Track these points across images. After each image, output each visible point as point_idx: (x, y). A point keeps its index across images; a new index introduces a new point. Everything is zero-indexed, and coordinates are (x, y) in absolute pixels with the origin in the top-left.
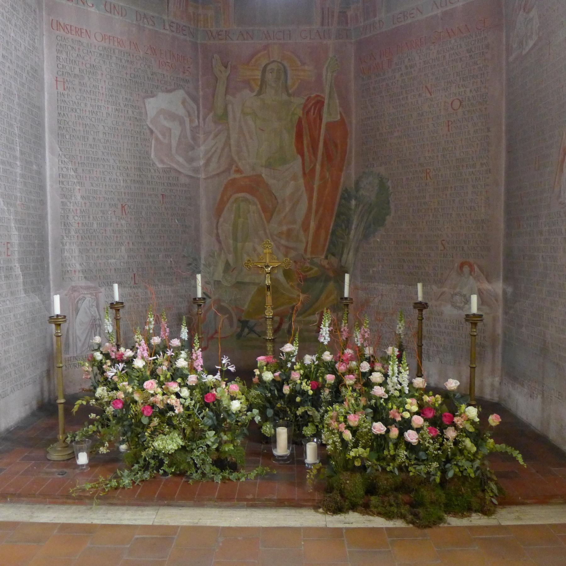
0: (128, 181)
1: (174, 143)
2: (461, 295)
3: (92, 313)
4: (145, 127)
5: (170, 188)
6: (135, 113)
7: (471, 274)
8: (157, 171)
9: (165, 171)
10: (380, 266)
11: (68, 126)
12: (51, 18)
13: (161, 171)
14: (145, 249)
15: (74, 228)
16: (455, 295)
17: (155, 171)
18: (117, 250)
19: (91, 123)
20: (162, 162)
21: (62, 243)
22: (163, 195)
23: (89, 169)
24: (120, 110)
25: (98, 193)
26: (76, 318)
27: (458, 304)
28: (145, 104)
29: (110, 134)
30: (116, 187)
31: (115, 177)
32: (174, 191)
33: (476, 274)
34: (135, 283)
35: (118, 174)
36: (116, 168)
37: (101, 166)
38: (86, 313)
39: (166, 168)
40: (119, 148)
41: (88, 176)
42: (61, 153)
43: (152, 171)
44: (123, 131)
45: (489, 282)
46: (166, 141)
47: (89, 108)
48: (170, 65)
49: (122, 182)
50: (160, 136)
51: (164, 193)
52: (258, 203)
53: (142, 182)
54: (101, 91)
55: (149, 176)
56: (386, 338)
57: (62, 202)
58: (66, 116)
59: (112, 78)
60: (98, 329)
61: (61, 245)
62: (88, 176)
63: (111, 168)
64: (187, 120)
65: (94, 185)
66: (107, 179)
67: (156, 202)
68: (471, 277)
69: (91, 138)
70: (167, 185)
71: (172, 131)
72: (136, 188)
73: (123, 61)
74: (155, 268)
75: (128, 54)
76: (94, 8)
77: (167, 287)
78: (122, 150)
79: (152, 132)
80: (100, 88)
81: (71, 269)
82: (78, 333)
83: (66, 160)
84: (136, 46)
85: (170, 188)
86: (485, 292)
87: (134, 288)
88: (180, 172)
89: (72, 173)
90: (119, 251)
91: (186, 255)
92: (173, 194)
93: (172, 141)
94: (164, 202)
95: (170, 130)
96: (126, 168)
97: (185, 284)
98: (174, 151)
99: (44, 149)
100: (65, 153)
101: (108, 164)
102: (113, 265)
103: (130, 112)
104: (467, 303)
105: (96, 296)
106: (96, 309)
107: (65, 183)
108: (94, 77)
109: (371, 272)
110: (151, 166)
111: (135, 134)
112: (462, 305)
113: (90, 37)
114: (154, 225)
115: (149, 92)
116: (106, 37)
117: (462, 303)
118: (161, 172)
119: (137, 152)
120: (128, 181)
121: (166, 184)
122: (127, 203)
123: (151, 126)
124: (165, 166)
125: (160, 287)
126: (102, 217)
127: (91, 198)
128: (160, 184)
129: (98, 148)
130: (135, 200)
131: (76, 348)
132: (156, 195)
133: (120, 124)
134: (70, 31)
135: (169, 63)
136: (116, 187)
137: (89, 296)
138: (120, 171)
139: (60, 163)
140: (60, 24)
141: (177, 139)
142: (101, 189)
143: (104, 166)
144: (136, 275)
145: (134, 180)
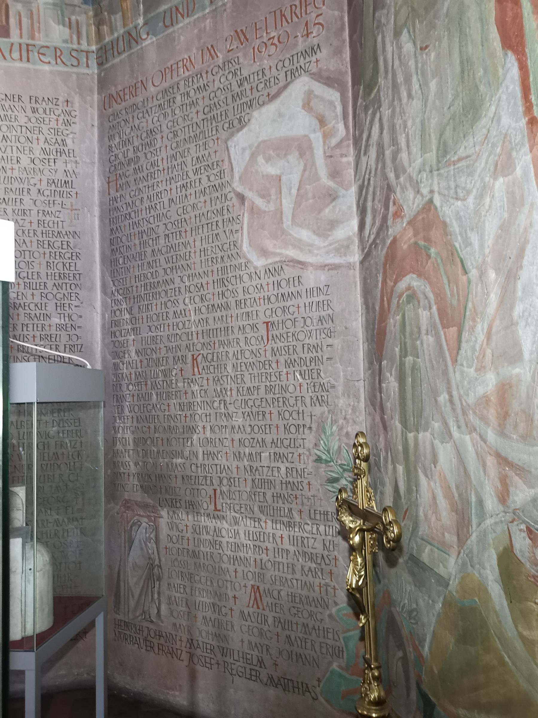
0: (204, 310)
1: (287, 205)
3: (150, 551)
4: (232, 194)
5: (282, 304)
6: (212, 178)
8: (254, 276)
9: (268, 271)
11: (121, 244)
12: (103, 95)
13: (263, 273)
14: (233, 440)
15: (127, 403)
17: (251, 277)
18: (185, 440)
19: (149, 225)
20: (264, 253)
21: (114, 428)
22: (267, 323)
23: (146, 303)
24: (189, 185)
25: (158, 341)
26: (129, 554)
28: (228, 150)
29: (174, 234)
30: (184, 325)
31: (182, 306)
32: (292, 309)
34: (216, 509)
35: (187, 301)
36: (183, 290)
37: (163, 294)
38: (142, 549)
39: (271, 264)
40: (187, 254)
41: (144, 315)
42: (114, 288)
43: (246, 278)
44: (193, 220)
46: (272, 207)
47: (147, 204)
48: (276, 41)
49: (192, 313)
50: (259, 202)
51: (271, 319)
52: (431, 296)
53: (228, 307)
54: (161, 168)
55: (240, 291)
57: (114, 364)
58: (119, 230)
59: (175, 135)
60: (157, 585)
61: (113, 432)
62: (144, 315)
63: (177, 293)
64: (317, 138)
65: (153, 329)
66: (171, 315)
67: (253, 341)
69: (149, 250)
70: (277, 299)
71: (284, 178)
72: (217, 319)
73: (192, 93)
74: (253, 481)
75: (199, 76)
76: (149, 37)
77: (278, 526)
78: (192, 255)
79: (242, 198)
80: (160, 163)
81: (125, 471)
82: (132, 581)
83: (120, 297)
84: (212, 51)
85: (282, 304)
87: (214, 518)
88: (302, 264)
89: (127, 316)
90: (189, 443)
91: (324, 457)
92: (290, 316)
93: (284, 201)
94: (270, 338)
95: (279, 178)
96: (199, 286)
97: (322, 528)
98: (287, 222)
99: (91, 289)
100: (119, 288)
101: (172, 286)
102: (179, 469)
103: (205, 180)
105: (154, 522)
106: (155, 546)
107: (118, 334)
108: (151, 150)
110: (243, 268)
111: (213, 216)
113: (146, 89)
114: (249, 389)
115: (236, 122)
116: (167, 70)
118: (262, 276)
119: (218, 251)
120: (204, 310)
121: (273, 299)
122: (202, 352)
123: (240, 189)
124: (270, 261)
125: (263, 524)
126: (163, 381)
127: (149, 351)
128: (262, 301)
129: (158, 264)
130: (214, 344)
131: (128, 608)
132: (254, 327)
133: (189, 208)
134: (122, 97)
135: (273, 38)
136: (184, 325)
137: (146, 520)
138: (191, 294)
139: (113, 304)
140: (112, 96)
141: (294, 191)
142: (162, 334)
143: (166, 292)
144: (218, 491)
145: (213, 306)
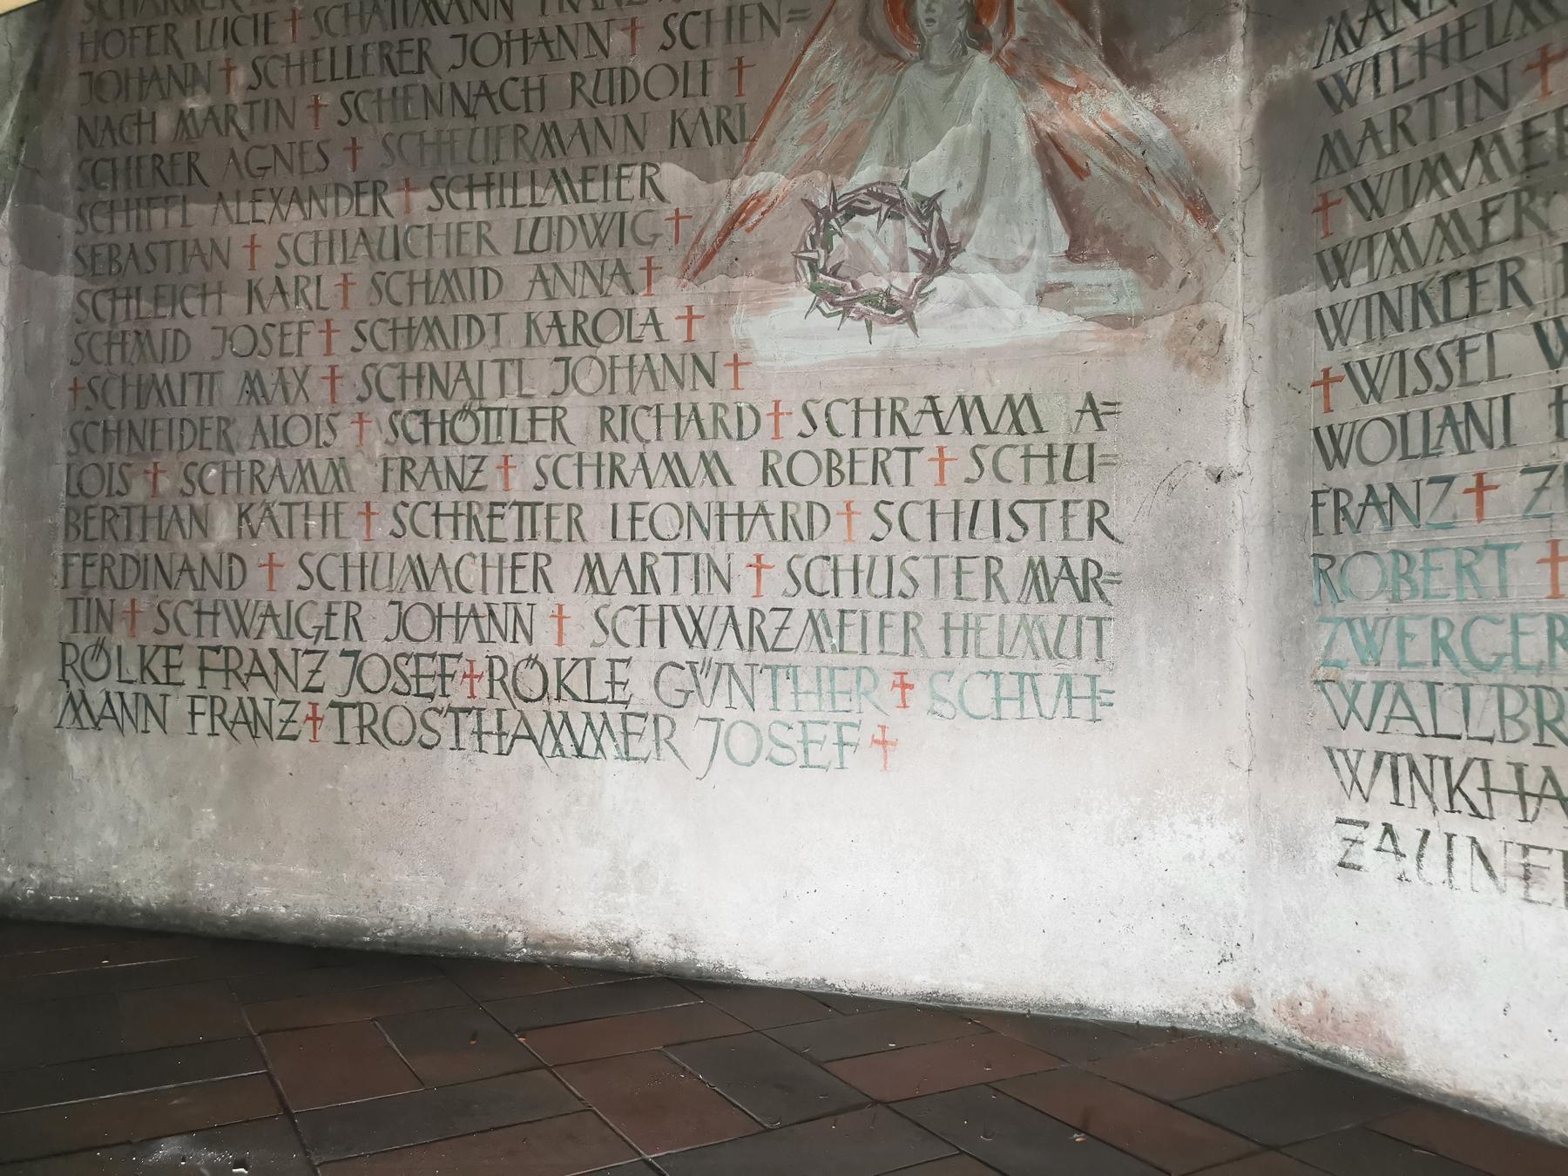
2: (896, 209)
7: (979, 38)
10: (241, 76)
16: (851, 212)
27: (868, 283)
33: (1019, 32)
45: (1135, 76)
56: (271, 613)
68: (981, 59)
86: (1097, 160)
104: (946, 267)
109: (165, 123)
112: (902, 284)
117: (903, 268)
